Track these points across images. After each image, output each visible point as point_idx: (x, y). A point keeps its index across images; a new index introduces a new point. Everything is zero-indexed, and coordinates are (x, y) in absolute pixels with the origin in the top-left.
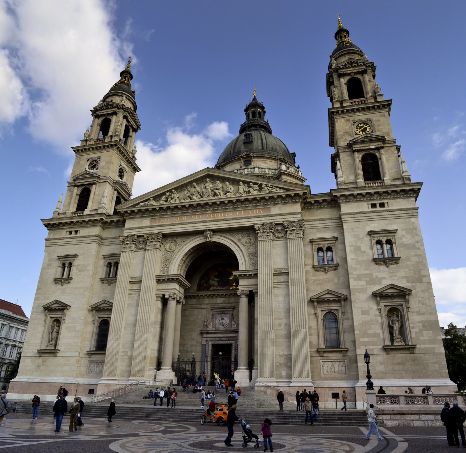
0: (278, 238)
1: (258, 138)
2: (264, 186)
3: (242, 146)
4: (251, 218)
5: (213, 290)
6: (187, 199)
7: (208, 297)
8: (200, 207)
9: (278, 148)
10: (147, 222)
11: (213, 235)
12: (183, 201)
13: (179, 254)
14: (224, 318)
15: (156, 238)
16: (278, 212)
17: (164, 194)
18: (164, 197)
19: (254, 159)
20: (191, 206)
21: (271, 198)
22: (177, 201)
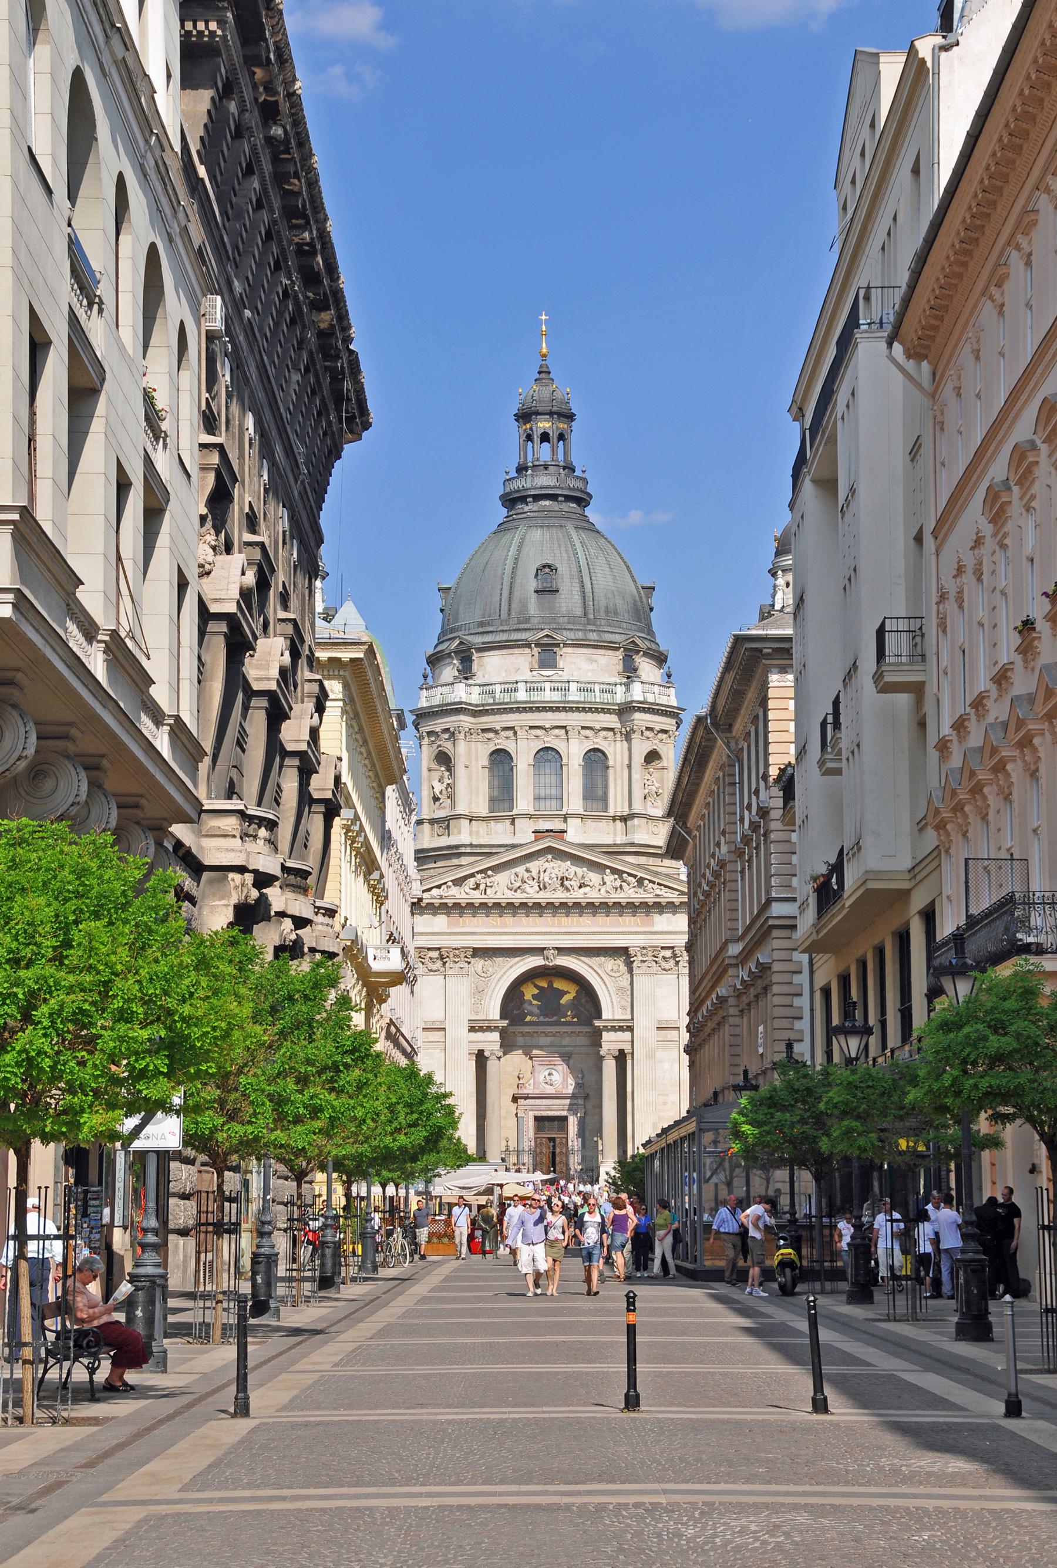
0: (664, 970)
1: (572, 577)
2: (646, 882)
3: (533, 600)
4: (623, 933)
5: (530, 1023)
6: (516, 891)
7: (523, 1036)
8: (539, 908)
9: (619, 602)
10: (441, 922)
11: (558, 955)
12: (509, 894)
13: (501, 981)
14: (554, 1072)
15: (462, 955)
16: (666, 929)
17: (472, 875)
18: (471, 882)
19: (566, 650)
20: (523, 905)
21: (657, 905)
22: (499, 895)
